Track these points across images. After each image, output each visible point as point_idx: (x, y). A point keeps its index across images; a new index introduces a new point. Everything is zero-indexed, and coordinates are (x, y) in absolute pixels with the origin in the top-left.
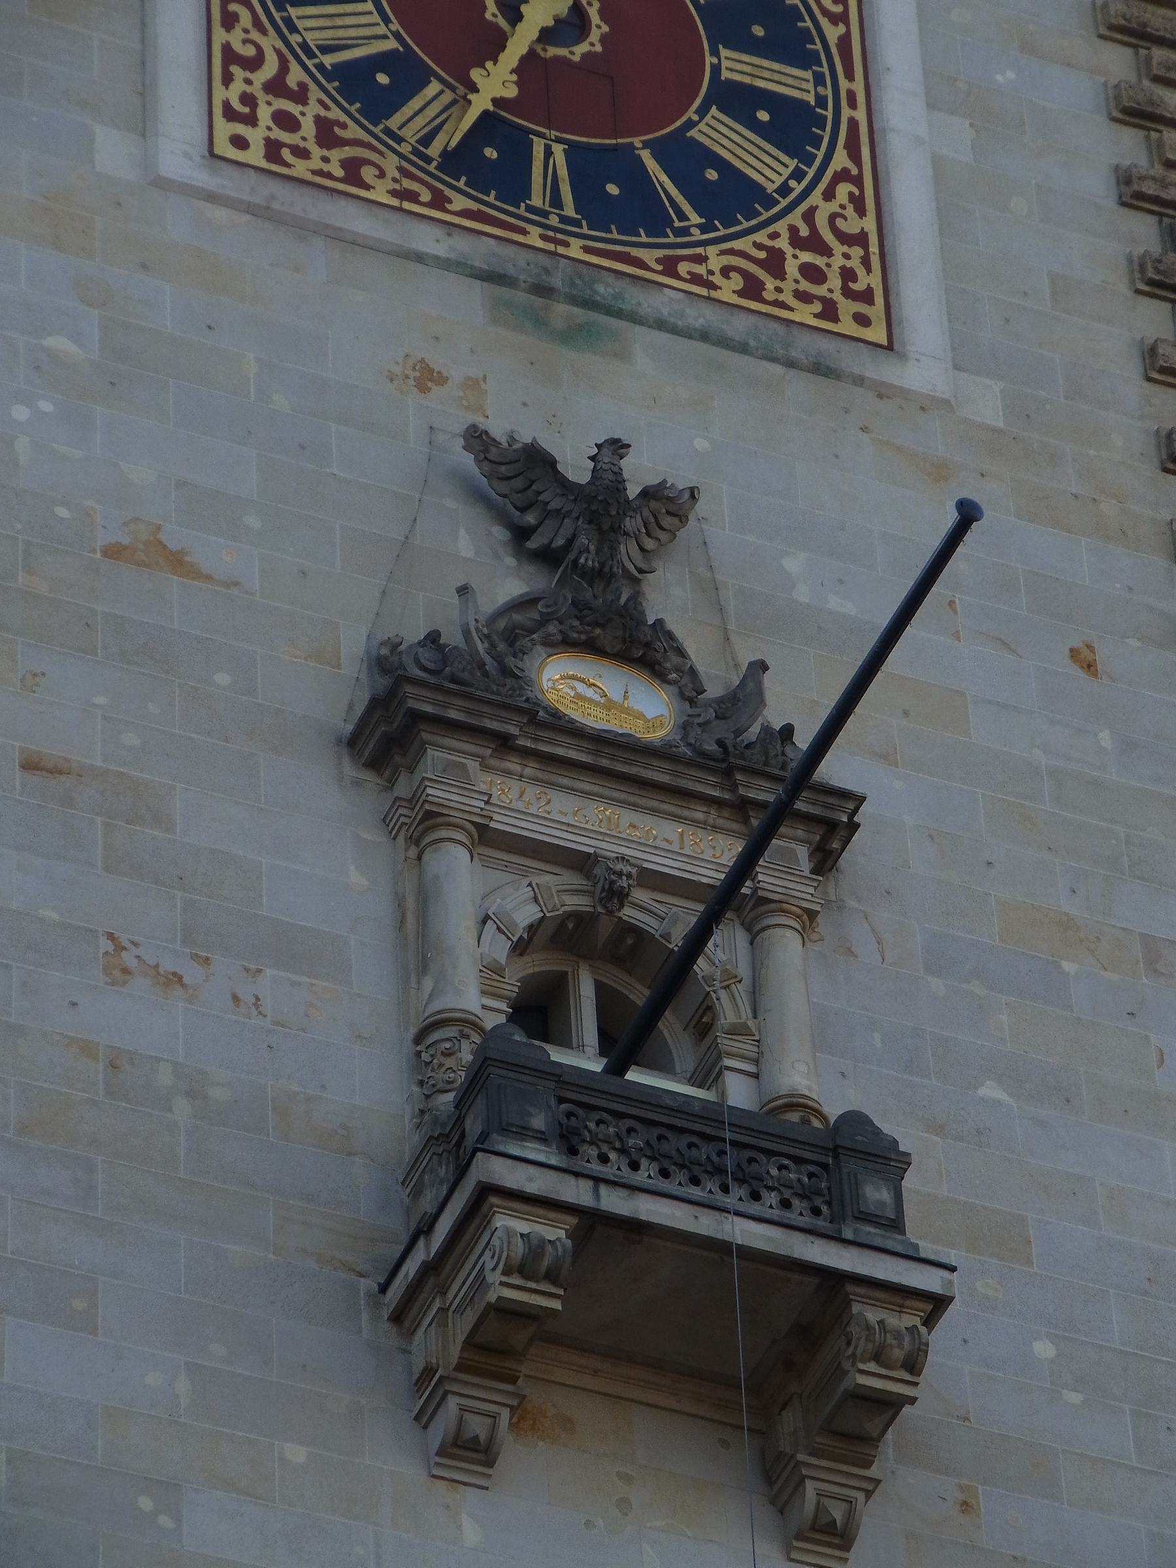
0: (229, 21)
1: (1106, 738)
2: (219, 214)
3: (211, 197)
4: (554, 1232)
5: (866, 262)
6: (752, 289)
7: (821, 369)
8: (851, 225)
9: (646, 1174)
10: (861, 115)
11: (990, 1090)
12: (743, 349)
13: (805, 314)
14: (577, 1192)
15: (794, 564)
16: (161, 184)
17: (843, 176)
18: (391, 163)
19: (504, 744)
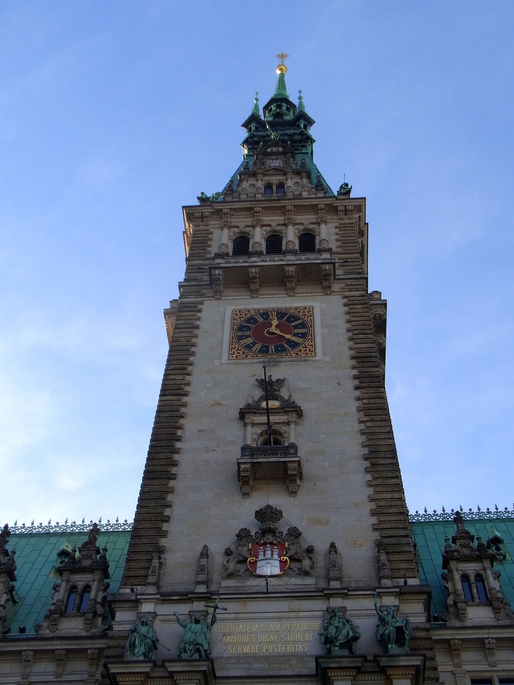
0: (232, 345)
1: (341, 392)
2: (229, 365)
3: (228, 364)
4: (248, 466)
5: (312, 348)
6: (297, 354)
7: (306, 361)
8: (311, 344)
9: (263, 456)
10: (313, 332)
11: (322, 436)
12: (295, 361)
13: (304, 355)
14: (250, 460)
15: (300, 383)
16: (222, 364)
17: (310, 339)
18: (251, 354)
19: (255, 413)
